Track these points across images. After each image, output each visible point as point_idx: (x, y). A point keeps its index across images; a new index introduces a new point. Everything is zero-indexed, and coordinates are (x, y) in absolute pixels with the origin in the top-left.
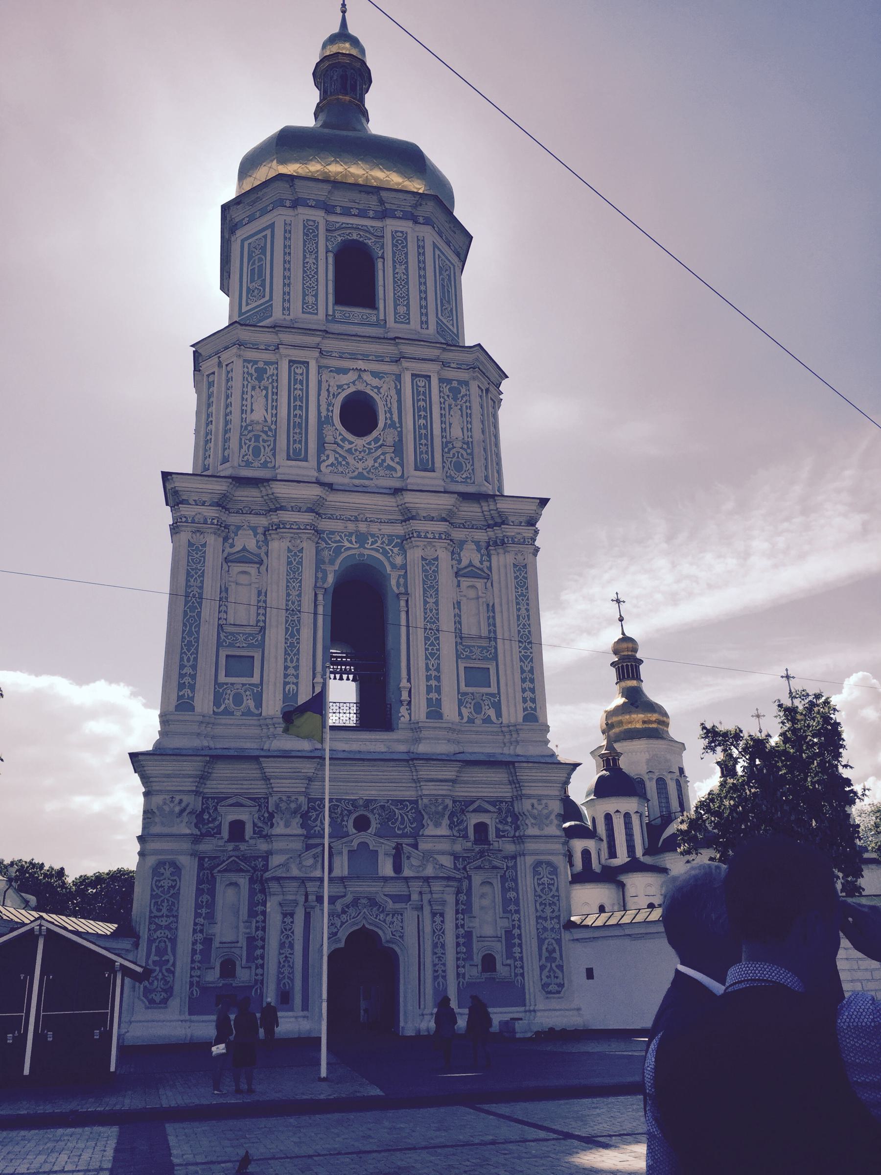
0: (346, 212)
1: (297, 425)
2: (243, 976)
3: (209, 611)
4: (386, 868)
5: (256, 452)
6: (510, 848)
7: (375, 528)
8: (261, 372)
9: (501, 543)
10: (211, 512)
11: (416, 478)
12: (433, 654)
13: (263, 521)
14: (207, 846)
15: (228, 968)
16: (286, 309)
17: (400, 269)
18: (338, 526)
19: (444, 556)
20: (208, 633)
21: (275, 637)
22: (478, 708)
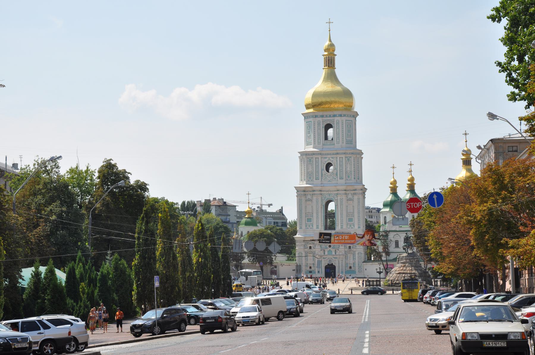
0: (326, 116)
1: (317, 172)
2: (313, 269)
3: (303, 211)
4: (334, 253)
5: (310, 178)
6: (355, 250)
7: (332, 192)
8: (310, 160)
9: (355, 194)
10: (303, 193)
11: (340, 181)
12: (342, 217)
13: (312, 193)
14: (306, 250)
15: (310, 268)
16: (314, 143)
17: (338, 130)
18: (325, 192)
19: (344, 197)
20: (304, 215)
21: (315, 215)
22: (350, 226)
